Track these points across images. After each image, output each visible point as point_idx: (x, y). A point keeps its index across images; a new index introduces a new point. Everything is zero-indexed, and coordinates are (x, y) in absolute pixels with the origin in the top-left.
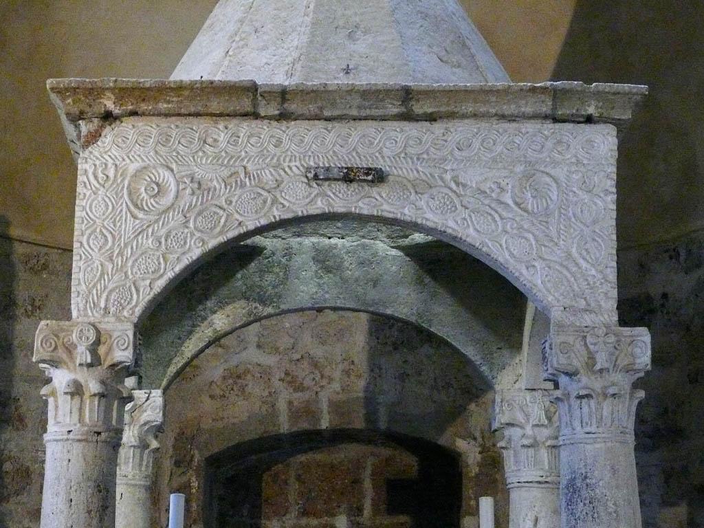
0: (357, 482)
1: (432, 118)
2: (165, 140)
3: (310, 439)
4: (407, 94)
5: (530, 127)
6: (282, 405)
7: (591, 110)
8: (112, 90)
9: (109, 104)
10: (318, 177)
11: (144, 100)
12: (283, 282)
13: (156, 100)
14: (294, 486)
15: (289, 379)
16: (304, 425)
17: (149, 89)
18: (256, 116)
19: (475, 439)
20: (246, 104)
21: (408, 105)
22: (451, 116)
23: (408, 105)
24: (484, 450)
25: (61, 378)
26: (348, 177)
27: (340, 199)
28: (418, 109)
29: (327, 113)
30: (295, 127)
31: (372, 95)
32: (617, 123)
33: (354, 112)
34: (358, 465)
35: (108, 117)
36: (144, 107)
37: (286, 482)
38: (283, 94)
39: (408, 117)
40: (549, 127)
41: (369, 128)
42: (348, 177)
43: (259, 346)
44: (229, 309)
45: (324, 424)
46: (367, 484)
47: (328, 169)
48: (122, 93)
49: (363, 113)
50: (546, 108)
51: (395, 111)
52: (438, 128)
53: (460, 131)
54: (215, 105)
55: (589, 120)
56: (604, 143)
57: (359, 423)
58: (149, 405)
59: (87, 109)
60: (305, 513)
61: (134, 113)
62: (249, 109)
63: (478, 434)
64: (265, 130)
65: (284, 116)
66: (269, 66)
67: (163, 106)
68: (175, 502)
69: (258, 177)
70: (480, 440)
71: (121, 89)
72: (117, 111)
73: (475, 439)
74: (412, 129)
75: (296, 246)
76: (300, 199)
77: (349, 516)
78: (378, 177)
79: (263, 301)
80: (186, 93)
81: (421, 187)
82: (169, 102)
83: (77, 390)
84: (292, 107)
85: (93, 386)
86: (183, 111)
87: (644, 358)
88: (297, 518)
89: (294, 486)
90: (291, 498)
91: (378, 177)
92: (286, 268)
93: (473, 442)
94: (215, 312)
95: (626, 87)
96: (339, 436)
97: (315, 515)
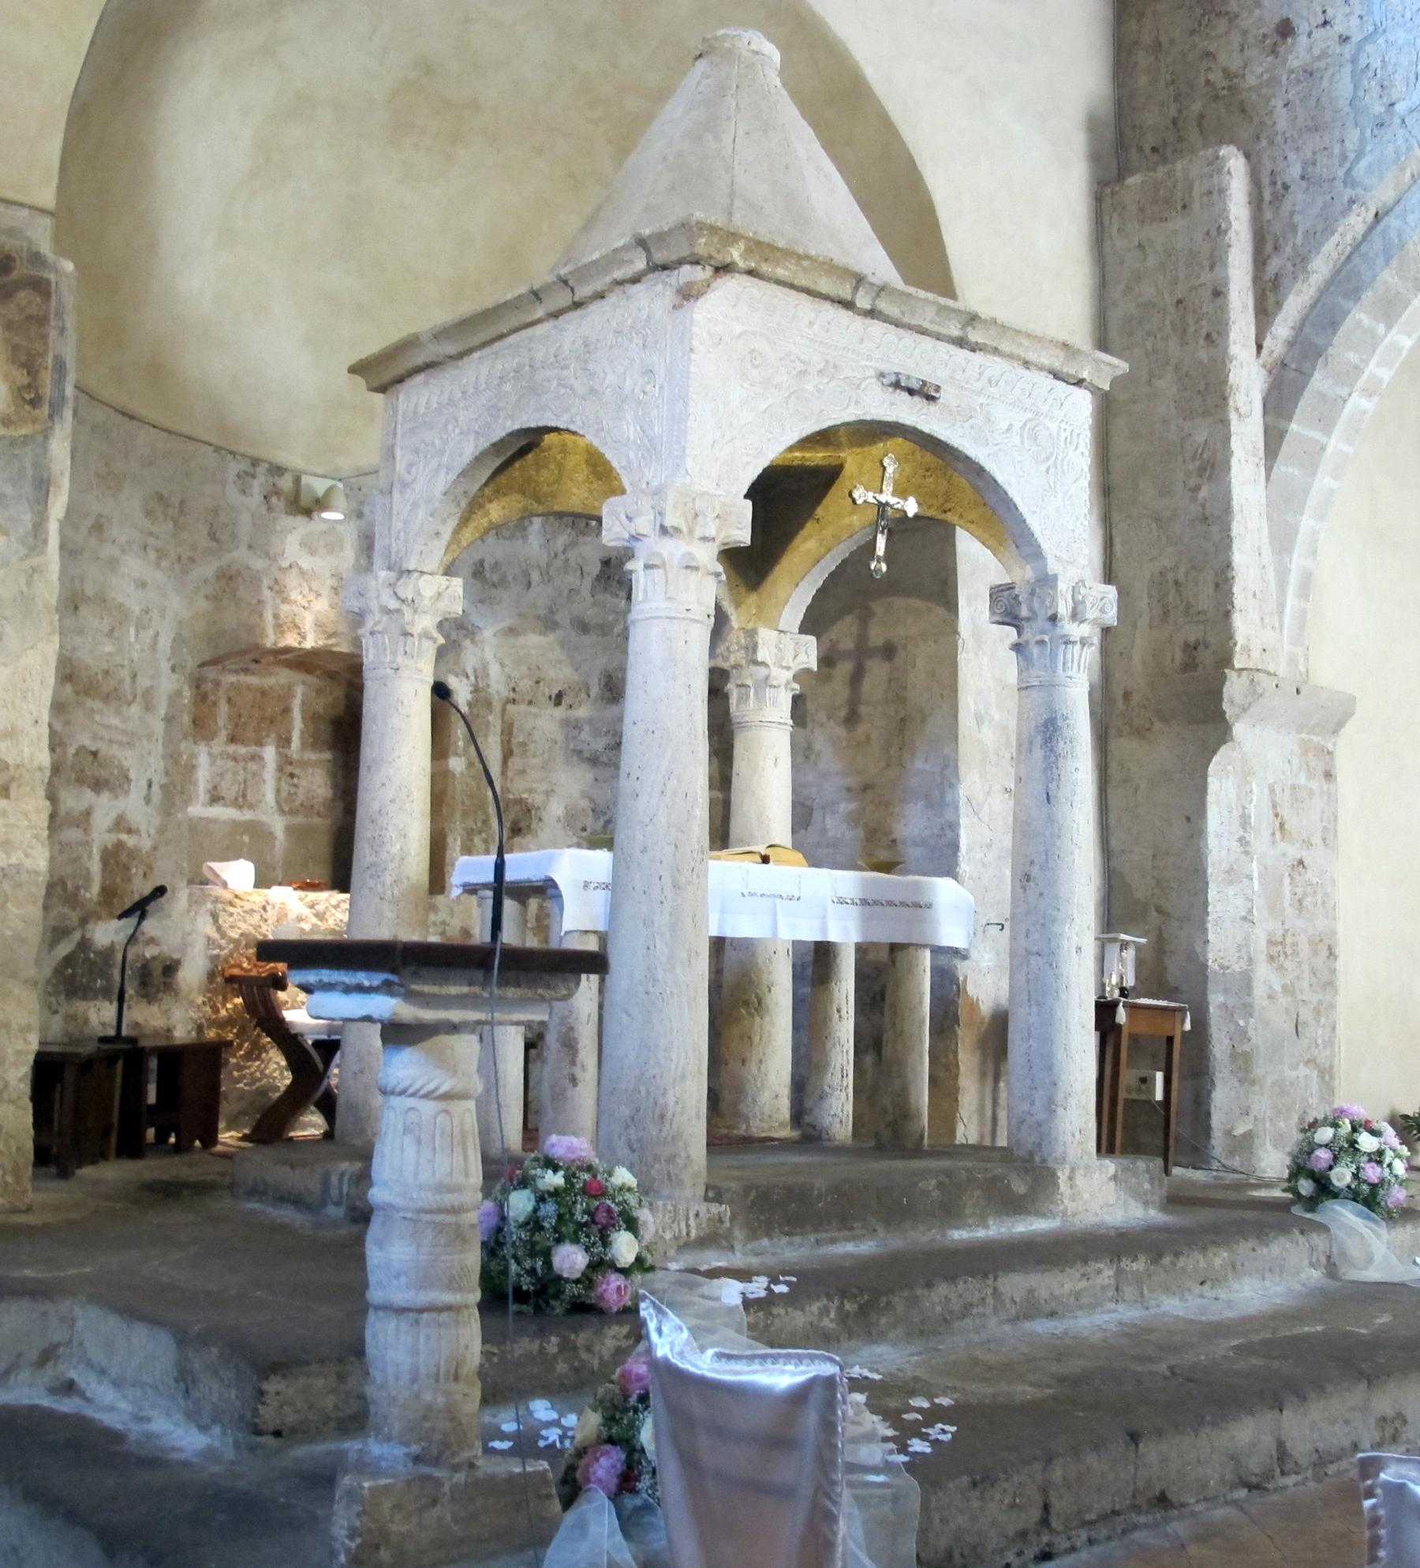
0: (287, 711)
7: (1085, 375)
8: (748, 239)
9: (736, 254)
11: (766, 260)
12: (558, 480)
13: (778, 263)
14: (224, 708)
15: (276, 588)
17: (778, 249)
18: (848, 305)
19: (467, 677)
20: (845, 292)
22: (996, 351)
24: (476, 690)
29: (906, 320)
30: (876, 327)
32: (1095, 390)
33: (926, 325)
34: (289, 689)
35: (724, 269)
36: (765, 268)
37: (215, 704)
39: (960, 342)
40: (1050, 381)
41: (927, 343)
43: (250, 547)
44: (504, 501)
47: (908, 377)
48: (759, 248)
49: (935, 328)
50: (1056, 364)
51: (955, 332)
52: (978, 357)
54: (825, 285)
55: (1079, 383)
59: (715, 254)
60: (233, 739)
61: (750, 273)
62: (849, 298)
63: (470, 672)
65: (871, 313)
67: (780, 272)
70: (472, 678)
71: (759, 244)
72: (741, 264)
73: (467, 677)
74: (963, 354)
75: (570, 444)
77: (277, 747)
79: (538, 500)
80: (805, 263)
82: (786, 268)
84: (883, 305)
86: (796, 282)
88: (226, 743)
89: (224, 708)
90: (221, 722)
92: (560, 465)
93: (465, 680)
94: (490, 501)
95: (1115, 361)
97: (243, 743)
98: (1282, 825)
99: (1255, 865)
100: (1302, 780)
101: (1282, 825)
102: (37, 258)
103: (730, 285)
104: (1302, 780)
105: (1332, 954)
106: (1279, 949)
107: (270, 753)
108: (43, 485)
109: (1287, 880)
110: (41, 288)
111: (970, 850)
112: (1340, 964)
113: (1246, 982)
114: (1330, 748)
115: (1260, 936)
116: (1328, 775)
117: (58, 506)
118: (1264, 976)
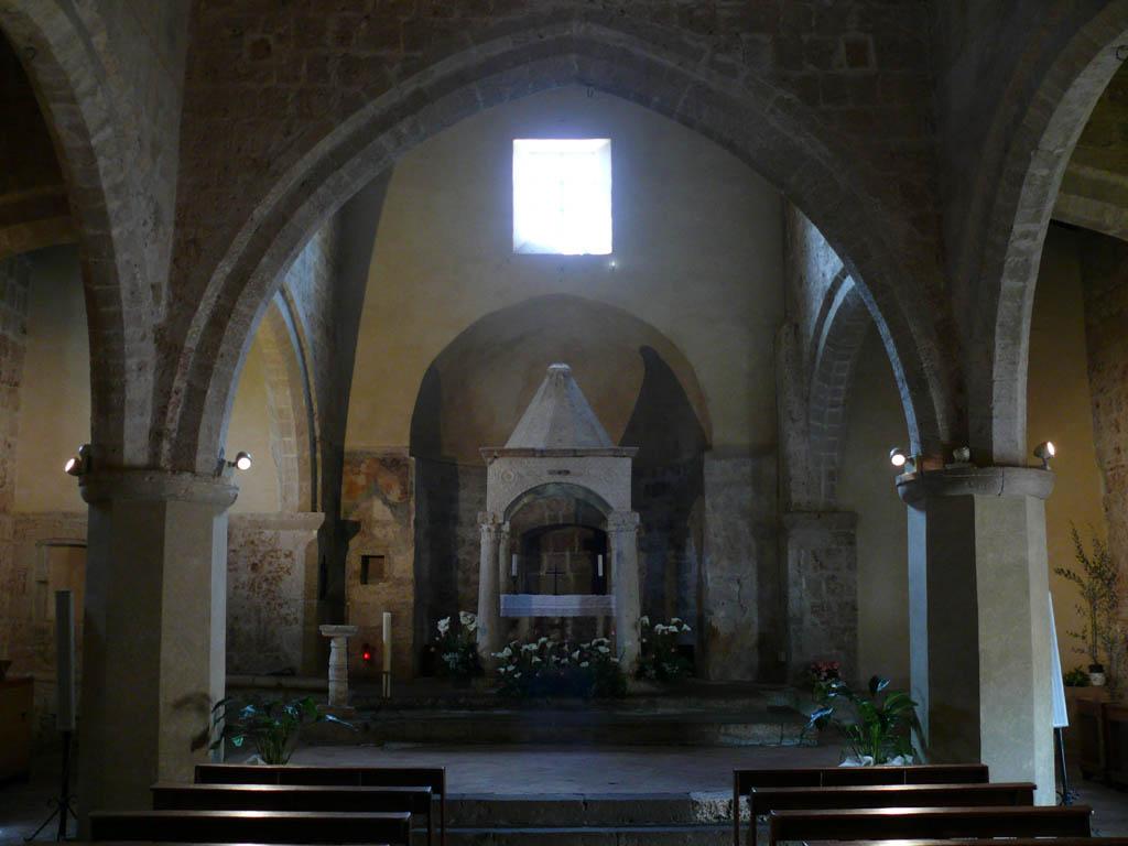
1: (581, 456)
2: (511, 463)
3: (558, 527)
4: (575, 451)
5: (608, 458)
6: (547, 514)
9: (496, 454)
10: (551, 472)
16: (552, 523)
21: (575, 453)
23: (575, 453)
25: (485, 527)
26: (560, 473)
27: (558, 478)
28: (579, 454)
31: (568, 451)
35: (496, 457)
38: (542, 451)
42: (560, 473)
45: (561, 522)
46: (576, 540)
52: (584, 459)
53: (590, 459)
56: (628, 462)
57: (573, 522)
58: (506, 527)
64: (537, 460)
66: (539, 443)
68: (515, 557)
69: (538, 472)
74: (577, 459)
76: (546, 479)
78: (567, 472)
81: (581, 475)
83: (489, 530)
85: (493, 529)
87: (638, 520)
91: (567, 472)
96: (564, 526)
98: (821, 564)
99: (803, 580)
100: (834, 546)
101: (821, 564)
102: (405, 459)
103: (496, 461)
104: (834, 546)
105: (854, 609)
106: (815, 610)
107: (568, 553)
108: (409, 513)
109: (824, 586)
110: (407, 466)
111: (712, 579)
112: (859, 613)
113: (800, 621)
114: (852, 532)
115: (807, 604)
116: (852, 543)
117: (413, 517)
118: (809, 619)
